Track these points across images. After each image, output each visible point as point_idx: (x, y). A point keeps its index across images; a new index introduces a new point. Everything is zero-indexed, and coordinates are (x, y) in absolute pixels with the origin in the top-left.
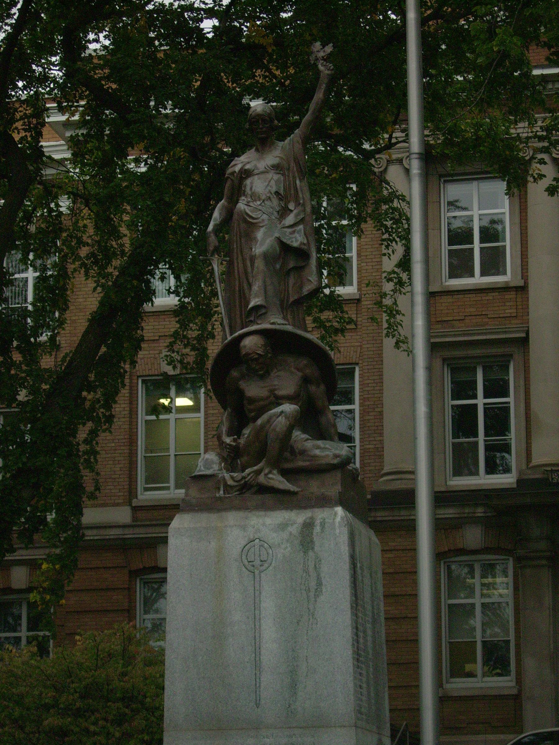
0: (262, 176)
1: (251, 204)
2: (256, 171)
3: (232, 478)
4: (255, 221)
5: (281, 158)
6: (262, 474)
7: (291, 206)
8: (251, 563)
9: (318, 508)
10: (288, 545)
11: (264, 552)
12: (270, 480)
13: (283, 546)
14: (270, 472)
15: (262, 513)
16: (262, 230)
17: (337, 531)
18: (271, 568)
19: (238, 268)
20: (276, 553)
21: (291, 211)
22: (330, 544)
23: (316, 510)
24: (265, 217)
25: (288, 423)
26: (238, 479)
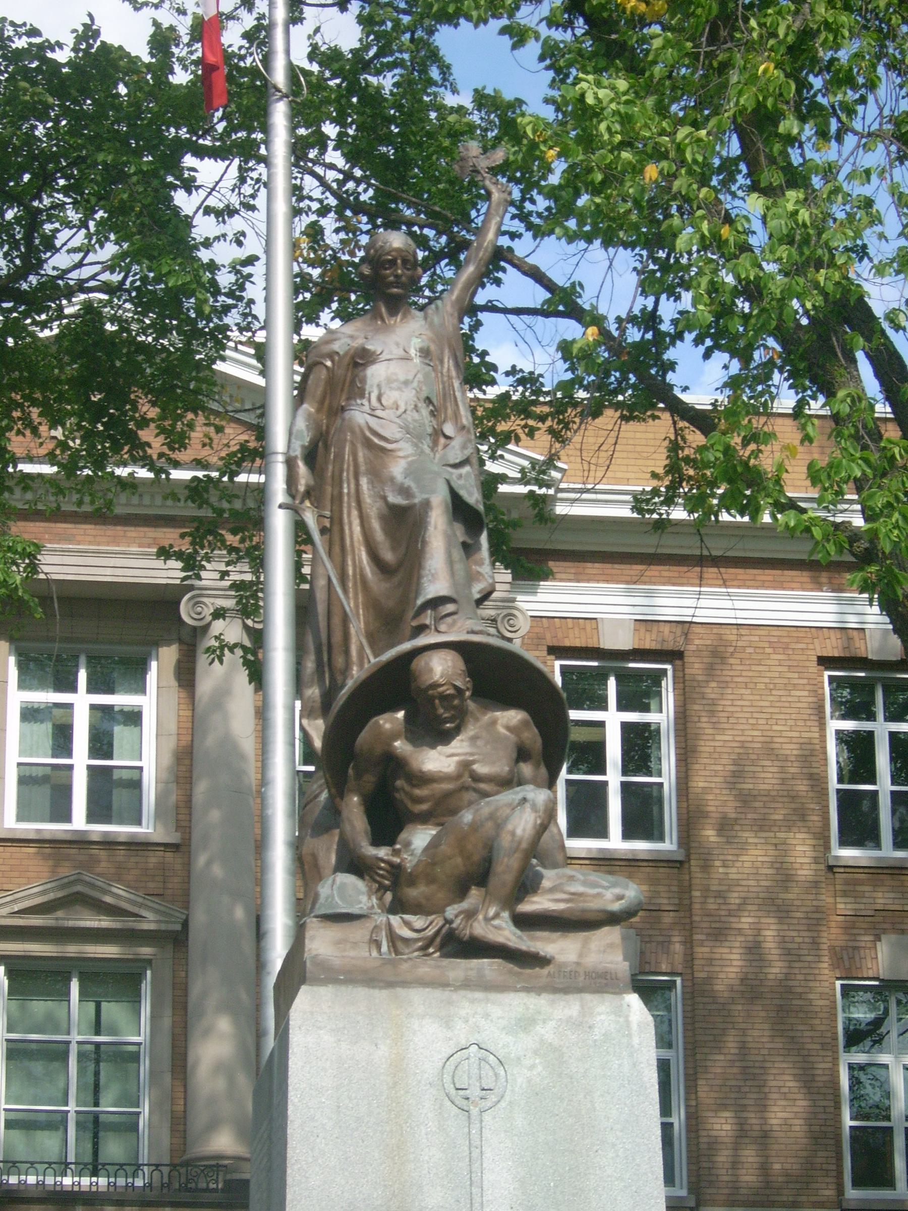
3: (407, 924)
8: (461, 1093)
10: (537, 1061)
11: (487, 1071)
13: (527, 1062)
14: (497, 916)
15: (479, 995)
17: (636, 1040)
18: (503, 1104)
20: (513, 1075)
22: (620, 1065)
23: (588, 997)
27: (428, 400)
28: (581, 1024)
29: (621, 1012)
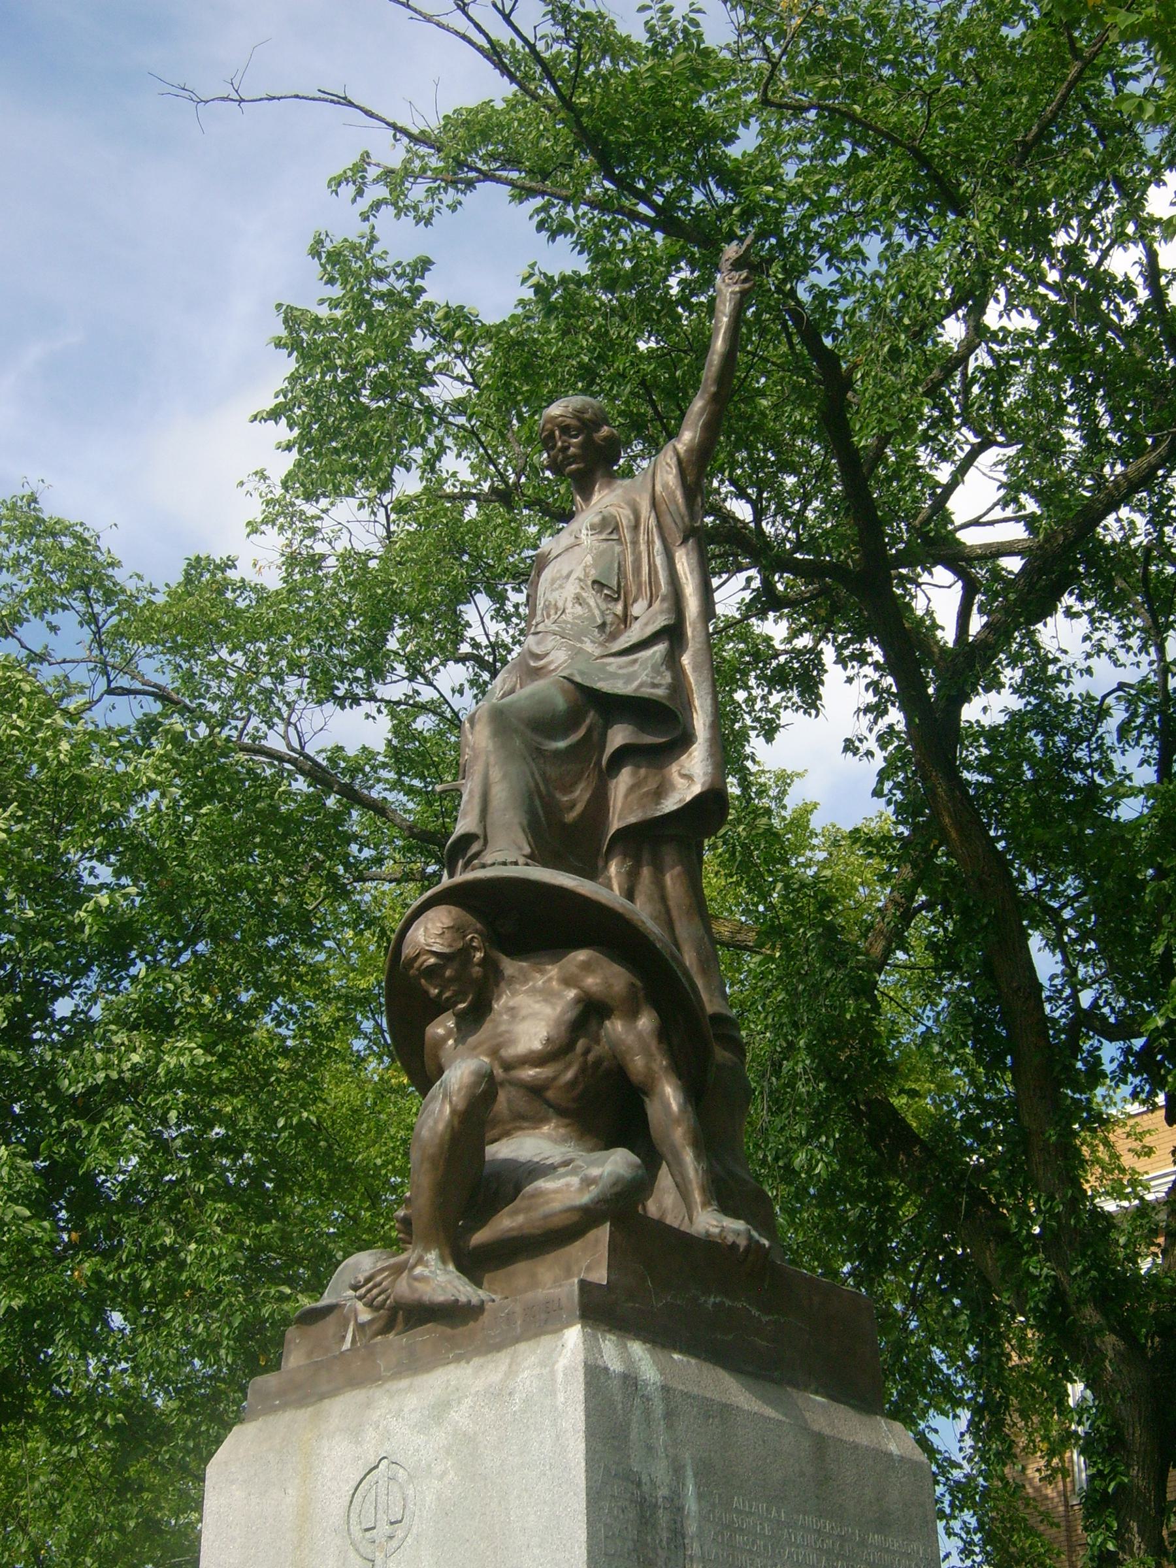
4: (542, 663)
12: (416, 1284)
13: (438, 1469)
17: (561, 1398)
27: (598, 584)
28: (499, 1394)
29: (548, 1362)
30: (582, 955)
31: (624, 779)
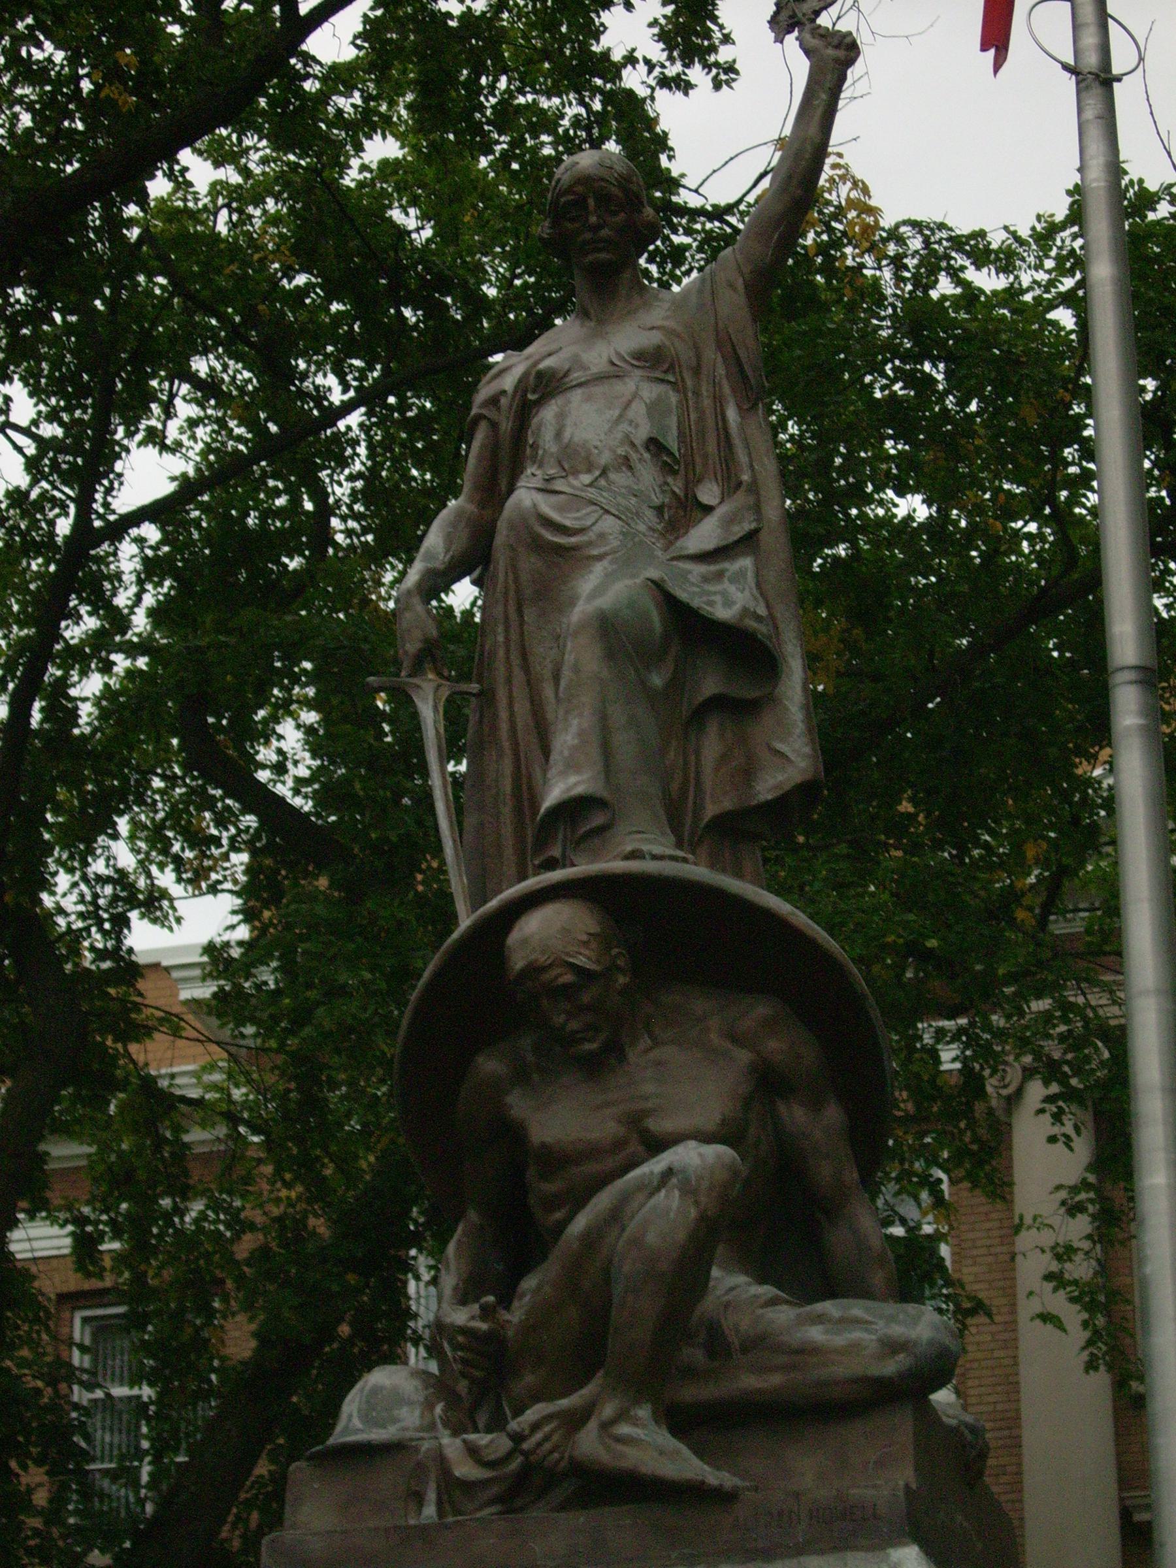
0: (598, 390)
1: (559, 485)
2: (577, 376)
3: (473, 1451)
4: (573, 540)
5: (669, 332)
6: (592, 1425)
7: (708, 493)
9: (822, 1552)
12: (620, 1447)
16: (598, 570)
19: (512, 715)
21: (708, 509)
24: (609, 524)
25: (693, 1213)
26: (492, 1457)
30: (762, 1009)
31: (712, 745)
